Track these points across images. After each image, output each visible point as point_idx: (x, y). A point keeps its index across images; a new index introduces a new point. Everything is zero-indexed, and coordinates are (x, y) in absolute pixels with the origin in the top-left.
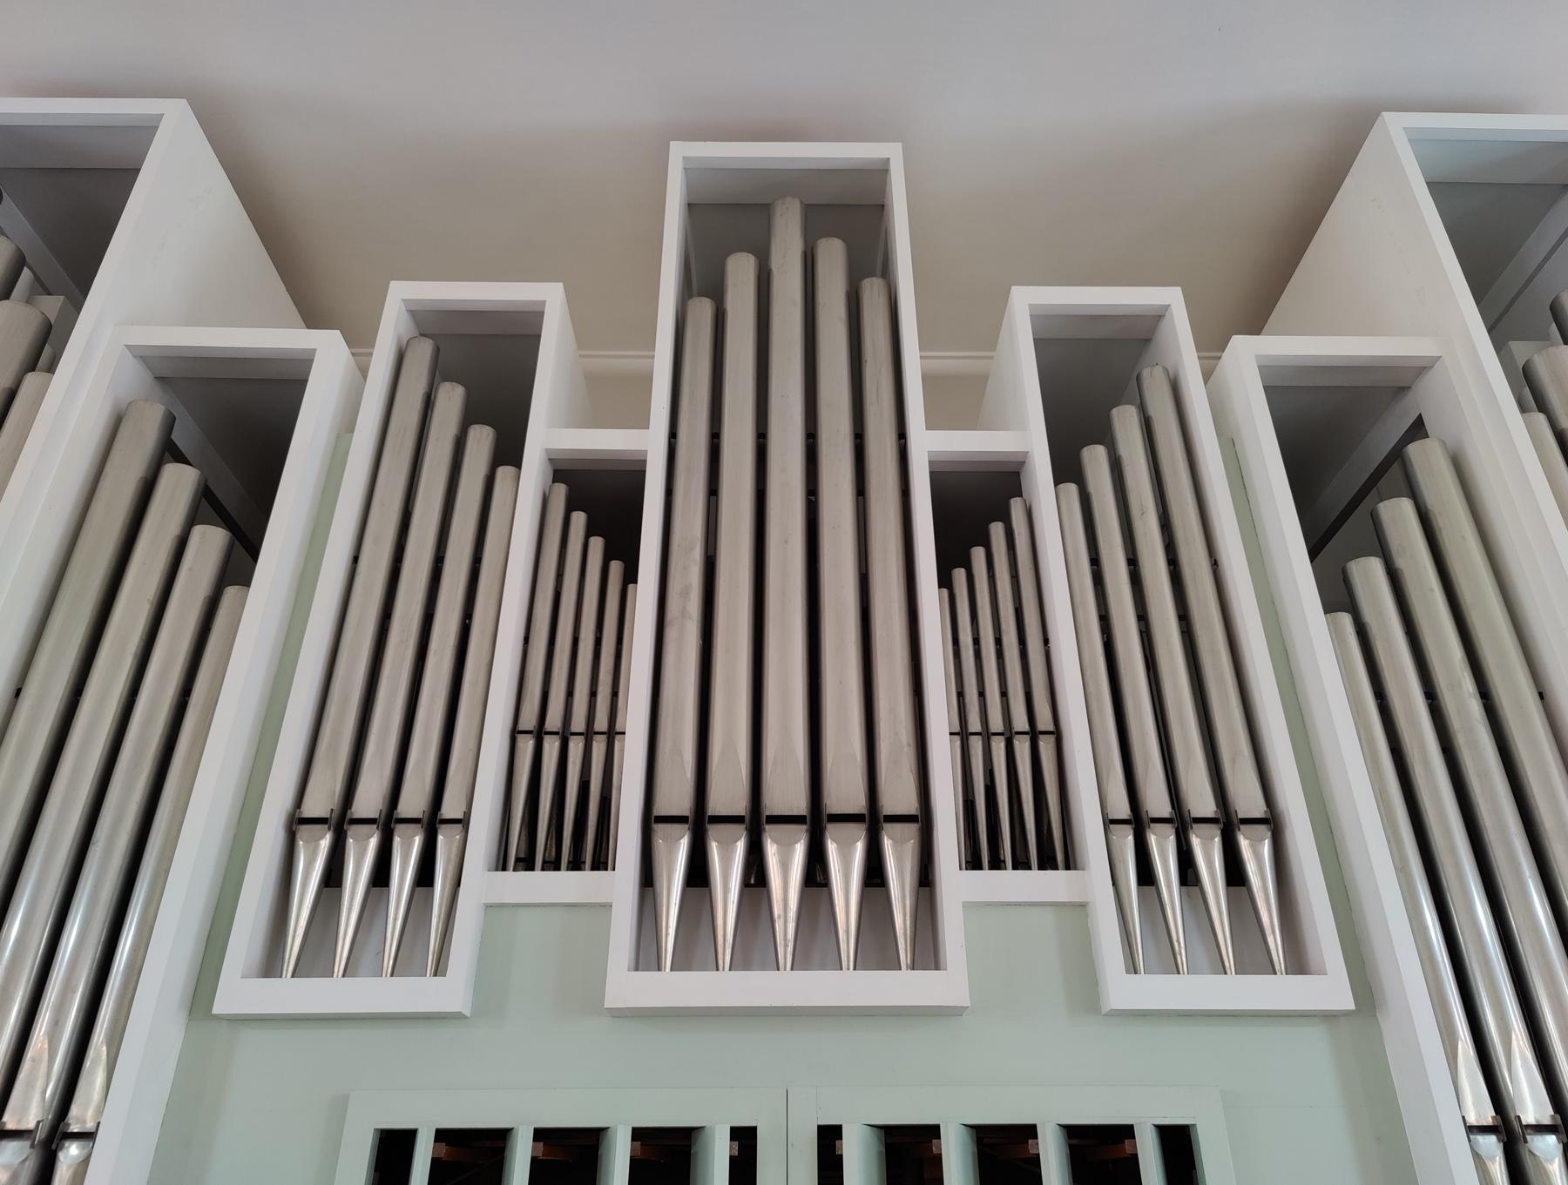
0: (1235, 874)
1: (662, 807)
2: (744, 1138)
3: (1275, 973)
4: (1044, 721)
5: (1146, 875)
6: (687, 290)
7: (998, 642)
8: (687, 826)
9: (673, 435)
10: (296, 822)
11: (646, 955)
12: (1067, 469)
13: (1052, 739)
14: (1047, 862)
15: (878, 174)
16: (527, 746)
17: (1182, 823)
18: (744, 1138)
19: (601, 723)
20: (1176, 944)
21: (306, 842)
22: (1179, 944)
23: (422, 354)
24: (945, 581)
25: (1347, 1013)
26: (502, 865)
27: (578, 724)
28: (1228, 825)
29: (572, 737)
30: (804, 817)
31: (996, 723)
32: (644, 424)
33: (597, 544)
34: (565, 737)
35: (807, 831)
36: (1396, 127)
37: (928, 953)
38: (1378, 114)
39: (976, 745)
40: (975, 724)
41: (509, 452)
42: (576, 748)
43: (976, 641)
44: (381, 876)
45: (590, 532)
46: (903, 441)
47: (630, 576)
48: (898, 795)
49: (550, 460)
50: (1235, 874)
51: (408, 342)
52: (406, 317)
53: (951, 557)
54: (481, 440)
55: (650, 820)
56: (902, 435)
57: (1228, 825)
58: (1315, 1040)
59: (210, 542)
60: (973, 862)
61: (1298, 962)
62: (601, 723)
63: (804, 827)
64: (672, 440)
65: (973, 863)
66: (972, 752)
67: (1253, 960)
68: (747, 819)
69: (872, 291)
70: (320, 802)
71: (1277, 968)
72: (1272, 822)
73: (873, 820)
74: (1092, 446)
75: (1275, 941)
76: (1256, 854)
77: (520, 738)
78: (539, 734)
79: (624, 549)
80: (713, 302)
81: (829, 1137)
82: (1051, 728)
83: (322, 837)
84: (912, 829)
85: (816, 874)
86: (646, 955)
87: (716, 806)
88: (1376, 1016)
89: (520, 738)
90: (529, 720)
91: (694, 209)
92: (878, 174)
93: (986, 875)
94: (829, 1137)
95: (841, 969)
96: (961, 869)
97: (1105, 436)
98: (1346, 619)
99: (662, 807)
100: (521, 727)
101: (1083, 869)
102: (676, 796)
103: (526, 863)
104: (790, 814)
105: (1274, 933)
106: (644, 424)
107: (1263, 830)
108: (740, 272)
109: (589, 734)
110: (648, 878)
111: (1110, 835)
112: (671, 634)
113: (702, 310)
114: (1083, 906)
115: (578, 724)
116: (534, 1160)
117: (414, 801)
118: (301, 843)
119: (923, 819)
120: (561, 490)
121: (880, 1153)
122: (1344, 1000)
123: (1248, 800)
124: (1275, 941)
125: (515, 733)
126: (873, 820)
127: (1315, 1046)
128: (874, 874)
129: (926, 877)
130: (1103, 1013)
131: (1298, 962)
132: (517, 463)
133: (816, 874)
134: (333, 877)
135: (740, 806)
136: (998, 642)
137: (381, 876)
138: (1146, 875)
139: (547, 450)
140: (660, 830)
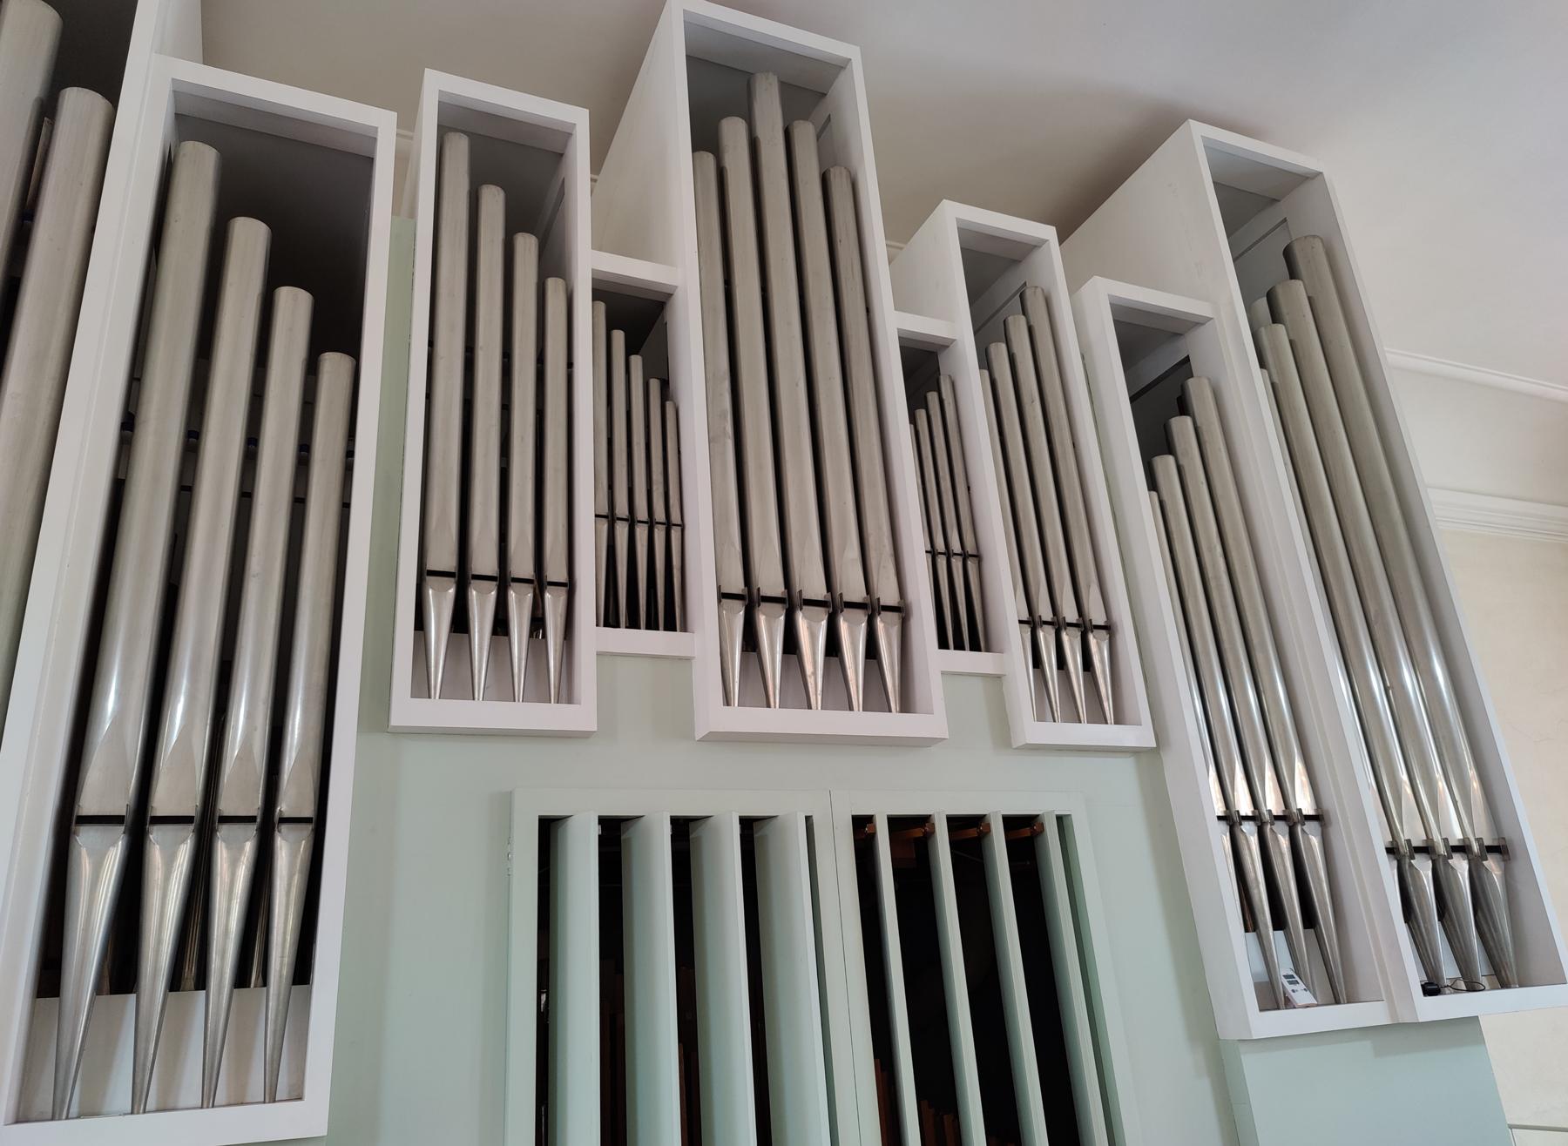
3: (1107, 723)
14: (975, 647)
36: (1197, 131)
38: (1185, 120)
39: (942, 561)
44: (501, 626)
58: (1127, 765)
67: (1098, 716)
70: (444, 556)
71: (1082, 719)
75: (1108, 706)
88: (1159, 753)
95: (851, 708)
101: (1001, 652)
107: (1103, 633)
114: (999, 677)
118: (474, 593)
124: (1108, 706)
127: (1125, 768)
130: (1014, 747)
134: (460, 623)
137: (501, 626)
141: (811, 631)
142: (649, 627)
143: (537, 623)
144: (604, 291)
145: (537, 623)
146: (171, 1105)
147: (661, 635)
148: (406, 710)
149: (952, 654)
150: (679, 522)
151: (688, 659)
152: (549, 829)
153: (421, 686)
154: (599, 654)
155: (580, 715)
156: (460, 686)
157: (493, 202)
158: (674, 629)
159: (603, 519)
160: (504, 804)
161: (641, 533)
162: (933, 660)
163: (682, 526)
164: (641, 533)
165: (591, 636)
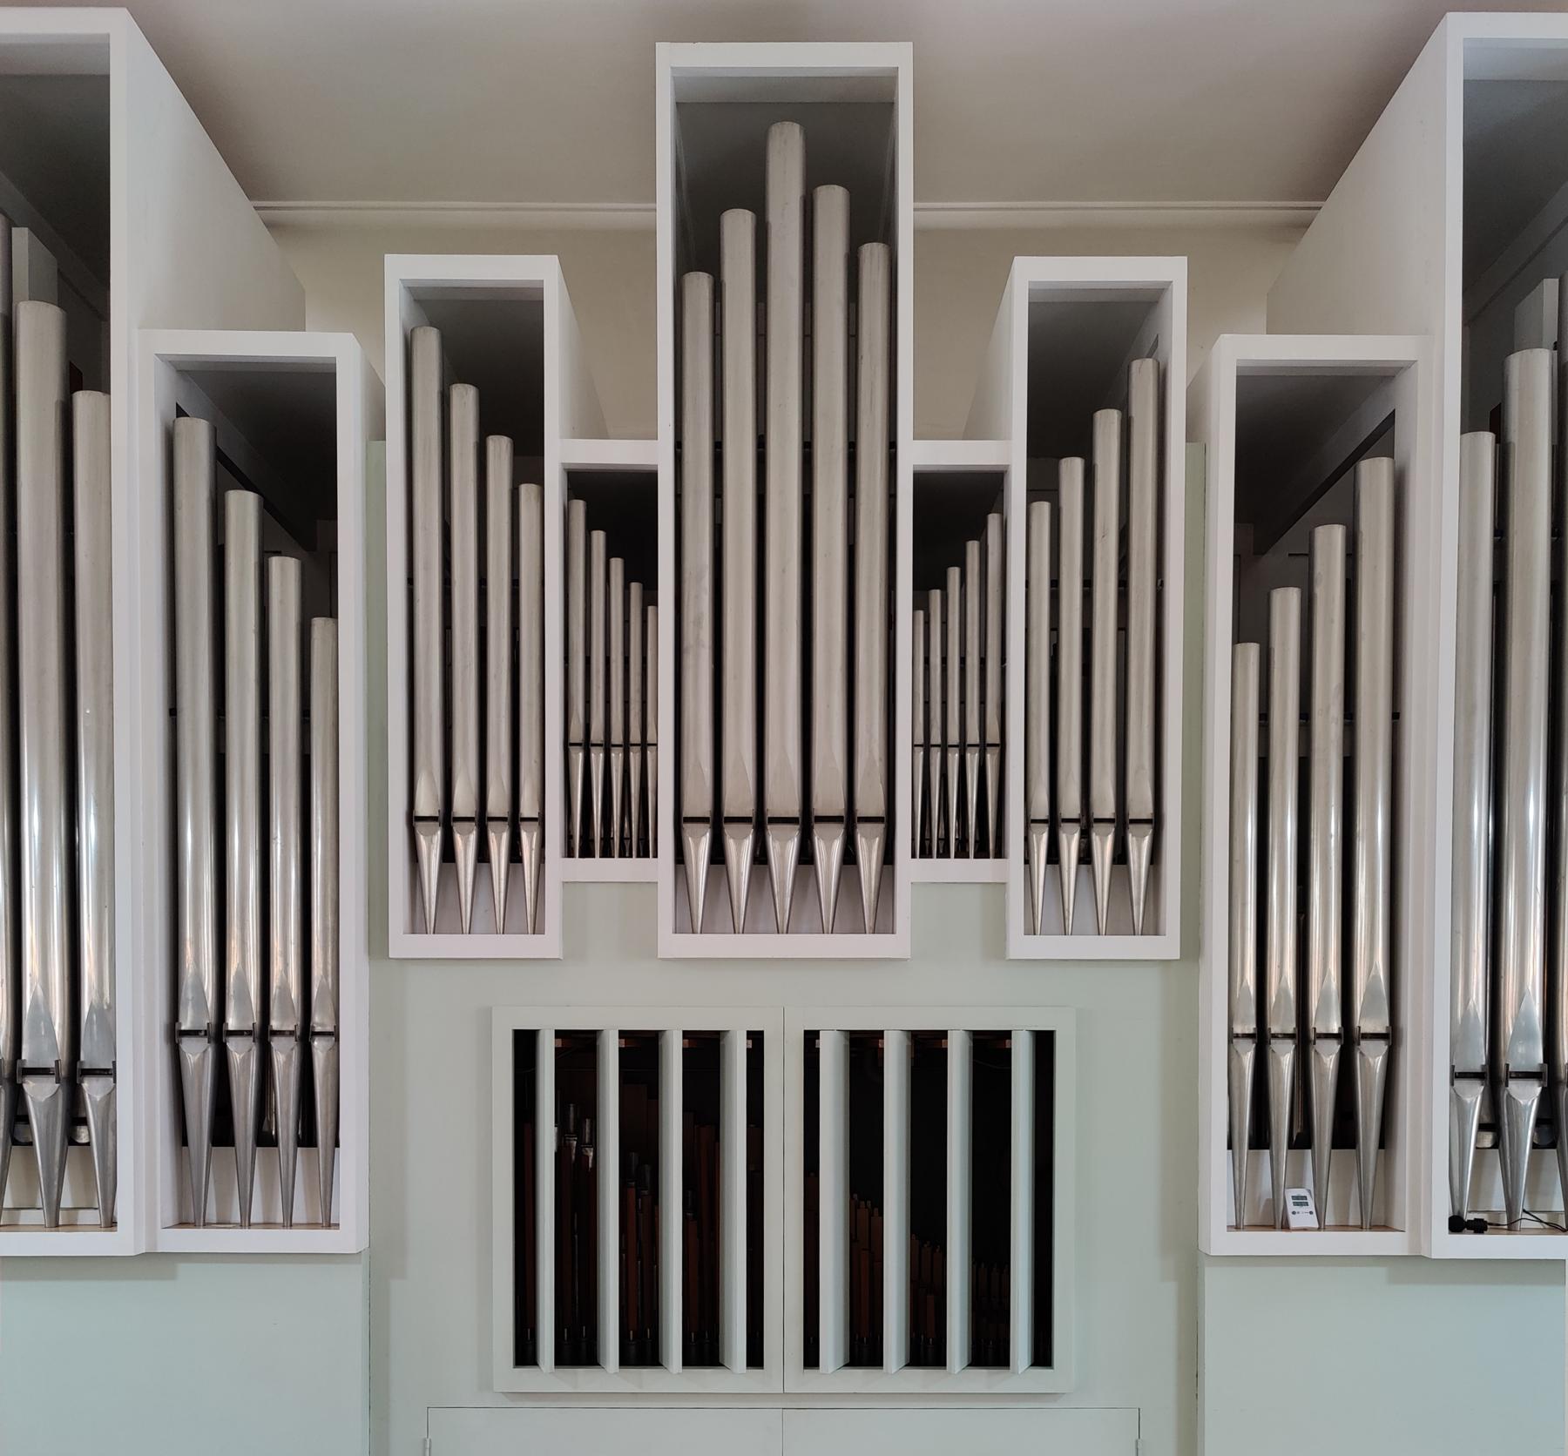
0: (1121, 856)
1: (688, 811)
2: (756, 1038)
4: (993, 735)
6: (684, 265)
7: (963, 661)
8: (708, 825)
9: (679, 445)
10: (412, 819)
11: (685, 923)
12: (1043, 487)
13: (997, 750)
14: (982, 852)
15: (888, 82)
16: (578, 757)
17: (1087, 823)
18: (756, 1038)
19: (635, 736)
20: (1066, 912)
21: (425, 835)
22: (1069, 912)
23: (429, 345)
24: (920, 603)
25: (1177, 960)
26: (569, 853)
27: (617, 737)
28: (1122, 822)
29: (613, 749)
30: (797, 819)
31: (954, 737)
32: (653, 436)
33: (617, 564)
34: (607, 747)
35: (799, 830)
37: (884, 922)
38: (1443, 15)
40: (936, 738)
41: (528, 465)
42: (617, 757)
43: (944, 660)
45: (610, 553)
46: (894, 450)
47: (650, 598)
48: (870, 801)
49: (565, 469)
50: (1121, 856)
51: (412, 330)
52: (403, 290)
53: (928, 579)
54: (500, 448)
55: (680, 820)
56: (892, 445)
57: (1122, 822)
59: (286, 572)
60: (924, 850)
61: (1153, 927)
62: (635, 736)
63: (798, 827)
64: (679, 450)
65: (925, 853)
66: (932, 761)
67: (1120, 924)
68: (754, 820)
69: (873, 254)
72: (1156, 822)
73: (850, 821)
74: (1069, 459)
76: (1139, 848)
77: (572, 749)
78: (587, 745)
79: (642, 571)
80: (711, 277)
81: (811, 1038)
82: (998, 742)
83: (435, 833)
84: (880, 828)
85: (806, 856)
86: (685, 923)
87: (729, 809)
89: (572, 749)
90: (577, 734)
91: (680, 107)
92: (888, 82)
93: (934, 863)
94: (811, 1038)
96: (913, 856)
97: (1084, 448)
98: (1252, 650)
99: (688, 811)
100: (572, 740)
102: (699, 801)
103: (587, 852)
104: (787, 816)
105: (1139, 904)
106: (653, 436)
108: (737, 227)
109: (626, 746)
110: (680, 857)
111: (1031, 833)
112: (688, 661)
113: (699, 284)
114: (1004, 884)
115: (617, 737)
116: (621, 1050)
117: (498, 803)
119: (889, 820)
120: (579, 507)
121: (845, 1046)
122: (1174, 953)
123: (1141, 804)
124: (1139, 909)
125: (567, 745)
126: (850, 821)
129: (888, 857)
130: (1007, 958)
131: (1153, 927)
132: (538, 479)
133: (806, 856)
135: (749, 810)
136: (963, 661)
139: (562, 464)
140: (688, 828)
142: (622, 855)
143: (515, 855)
144: (580, 482)
145: (515, 855)
146: (272, 1221)
148: (402, 943)
151: (657, 883)
153: (416, 925)
154: (564, 883)
155: (548, 944)
156: (449, 919)
157: (465, 399)
159: (578, 747)
160: (485, 1018)
164: (617, 757)
165: (559, 867)
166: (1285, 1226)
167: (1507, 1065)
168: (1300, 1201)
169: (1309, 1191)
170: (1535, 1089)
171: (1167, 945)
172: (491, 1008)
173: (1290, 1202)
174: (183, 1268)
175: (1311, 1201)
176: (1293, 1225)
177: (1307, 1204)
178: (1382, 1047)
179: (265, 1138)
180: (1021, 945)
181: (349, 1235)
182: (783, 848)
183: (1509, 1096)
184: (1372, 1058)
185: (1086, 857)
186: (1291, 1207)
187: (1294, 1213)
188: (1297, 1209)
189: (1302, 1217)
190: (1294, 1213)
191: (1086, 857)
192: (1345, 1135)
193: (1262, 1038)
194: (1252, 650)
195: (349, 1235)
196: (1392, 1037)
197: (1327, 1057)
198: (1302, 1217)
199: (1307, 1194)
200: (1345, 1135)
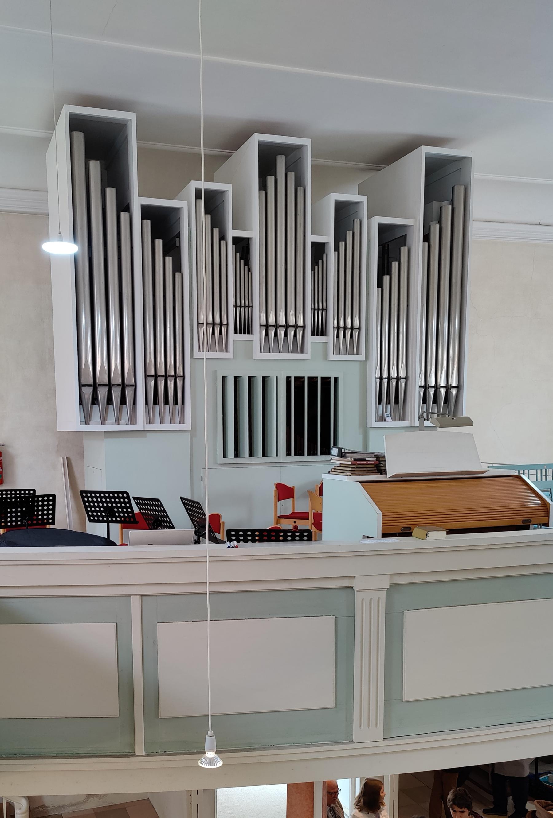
0: (352, 336)
5: (338, 336)
14: (322, 335)
48: (301, 323)
50: (352, 336)
58: (358, 364)
76: (356, 334)
98: (380, 289)
101: (328, 336)
114: (327, 342)
119: (304, 327)
128: (295, 335)
138: (338, 336)
141: (282, 332)
147: (246, 335)
148: (197, 354)
149: (316, 337)
150: (251, 306)
152: (224, 378)
155: (230, 355)
158: (249, 334)
160: (215, 372)
161: (242, 310)
162: (310, 339)
163: (252, 307)
165: (232, 336)
166: (385, 421)
167: (429, 385)
168: (388, 416)
169: (389, 413)
170: (433, 389)
171: (362, 357)
172: (216, 371)
173: (386, 416)
174: (148, 434)
175: (390, 415)
176: (387, 421)
177: (389, 416)
178: (404, 380)
179: (166, 402)
180: (332, 357)
181: (188, 426)
182: (282, 332)
183: (428, 391)
184: (402, 383)
185: (344, 336)
186: (386, 417)
187: (387, 418)
188: (387, 417)
189: (389, 419)
190: (387, 418)
191: (344, 336)
192: (397, 401)
193: (381, 378)
194: (380, 289)
195: (188, 426)
196: (406, 378)
197: (394, 383)
198: (389, 419)
199: (388, 414)
200: (397, 401)
